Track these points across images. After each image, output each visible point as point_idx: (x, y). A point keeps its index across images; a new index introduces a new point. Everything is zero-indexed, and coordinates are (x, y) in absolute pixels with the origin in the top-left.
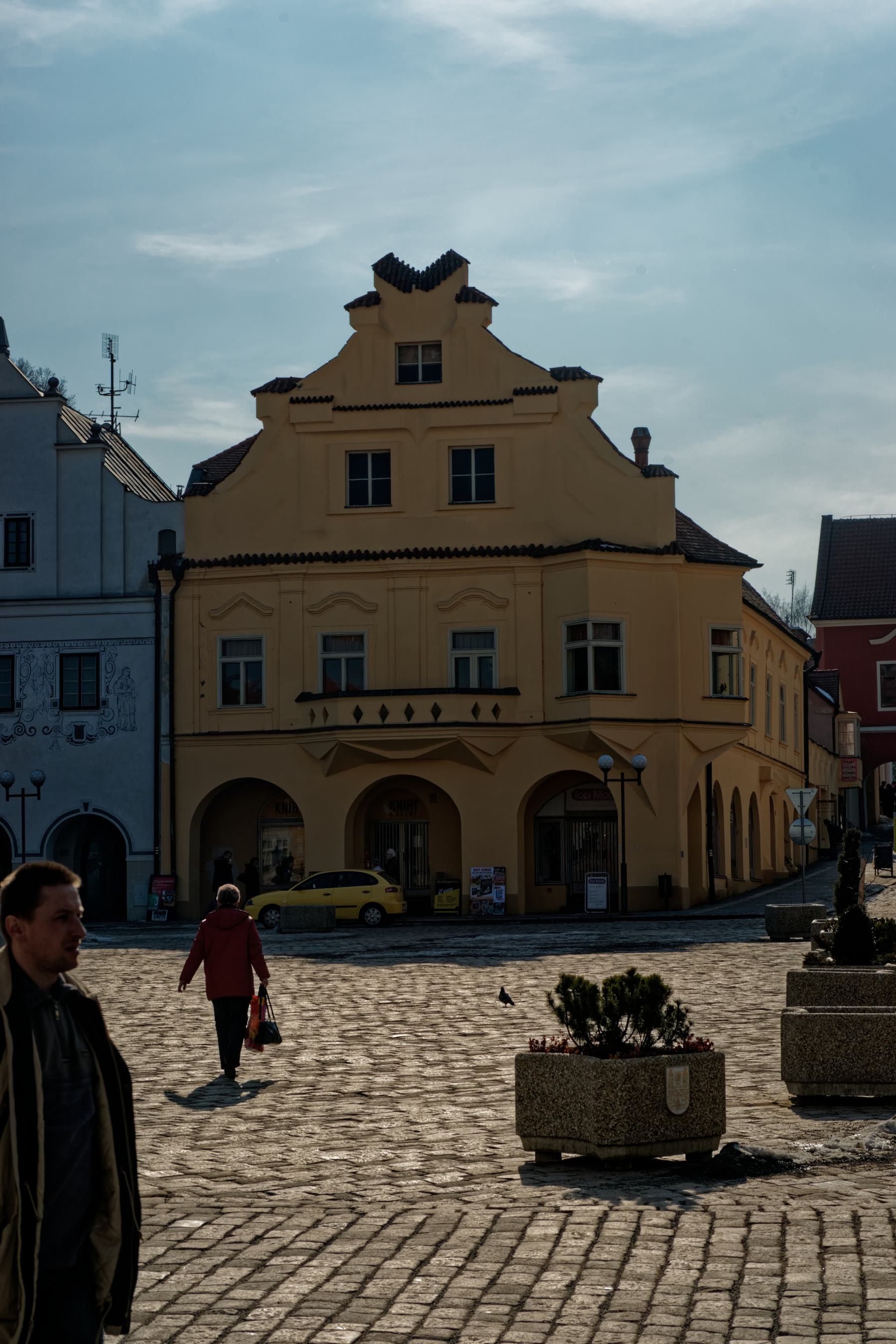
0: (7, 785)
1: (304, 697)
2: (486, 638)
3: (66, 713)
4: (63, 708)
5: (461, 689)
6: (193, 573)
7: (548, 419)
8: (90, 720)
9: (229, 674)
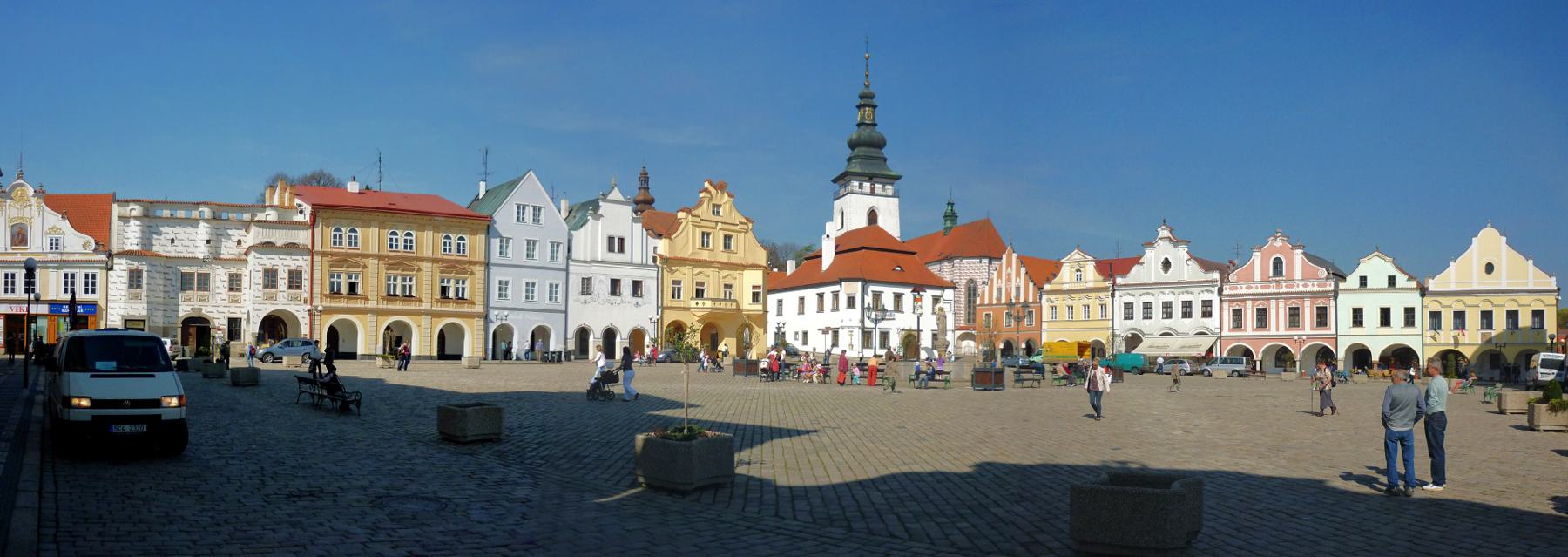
0: (651, 319)
1: (692, 299)
2: (730, 286)
5: (725, 300)
8: (639, 300)
9: (674, 289)
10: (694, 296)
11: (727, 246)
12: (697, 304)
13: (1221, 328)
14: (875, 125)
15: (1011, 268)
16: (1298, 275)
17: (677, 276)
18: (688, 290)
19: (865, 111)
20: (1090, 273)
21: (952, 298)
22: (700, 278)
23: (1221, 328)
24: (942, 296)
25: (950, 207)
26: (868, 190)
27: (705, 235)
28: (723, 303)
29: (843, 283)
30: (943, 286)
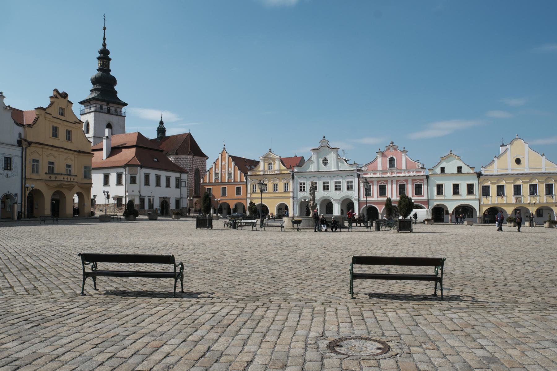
3: (5, 170)
4: (4, 169)
6: (33, 145)
7: (78, 128)
10: (47, 172)
11: (69, 138)
12: (50, 177)
13: (359, 197)
14: (110, 71)
15: (225, 162)
16: (404, 167)
17: (36, 157)
18: (44, 168)
19: (103, 62)
20: (277, 166)
21: (187, 179)
22: (51, 159)
23: (359, 197)
24: (181, 177)
25: (161, 125)
26: (106, 111)
27: (55, 129)
28: (66, 177)
29: (127, 168)
30: (182, 171)
